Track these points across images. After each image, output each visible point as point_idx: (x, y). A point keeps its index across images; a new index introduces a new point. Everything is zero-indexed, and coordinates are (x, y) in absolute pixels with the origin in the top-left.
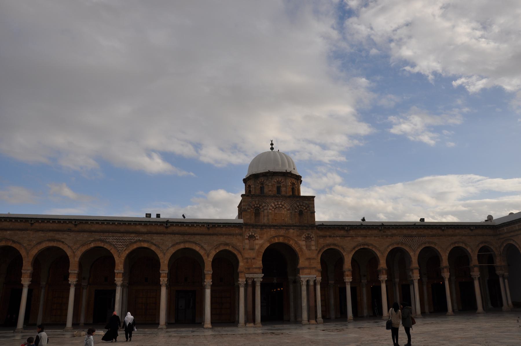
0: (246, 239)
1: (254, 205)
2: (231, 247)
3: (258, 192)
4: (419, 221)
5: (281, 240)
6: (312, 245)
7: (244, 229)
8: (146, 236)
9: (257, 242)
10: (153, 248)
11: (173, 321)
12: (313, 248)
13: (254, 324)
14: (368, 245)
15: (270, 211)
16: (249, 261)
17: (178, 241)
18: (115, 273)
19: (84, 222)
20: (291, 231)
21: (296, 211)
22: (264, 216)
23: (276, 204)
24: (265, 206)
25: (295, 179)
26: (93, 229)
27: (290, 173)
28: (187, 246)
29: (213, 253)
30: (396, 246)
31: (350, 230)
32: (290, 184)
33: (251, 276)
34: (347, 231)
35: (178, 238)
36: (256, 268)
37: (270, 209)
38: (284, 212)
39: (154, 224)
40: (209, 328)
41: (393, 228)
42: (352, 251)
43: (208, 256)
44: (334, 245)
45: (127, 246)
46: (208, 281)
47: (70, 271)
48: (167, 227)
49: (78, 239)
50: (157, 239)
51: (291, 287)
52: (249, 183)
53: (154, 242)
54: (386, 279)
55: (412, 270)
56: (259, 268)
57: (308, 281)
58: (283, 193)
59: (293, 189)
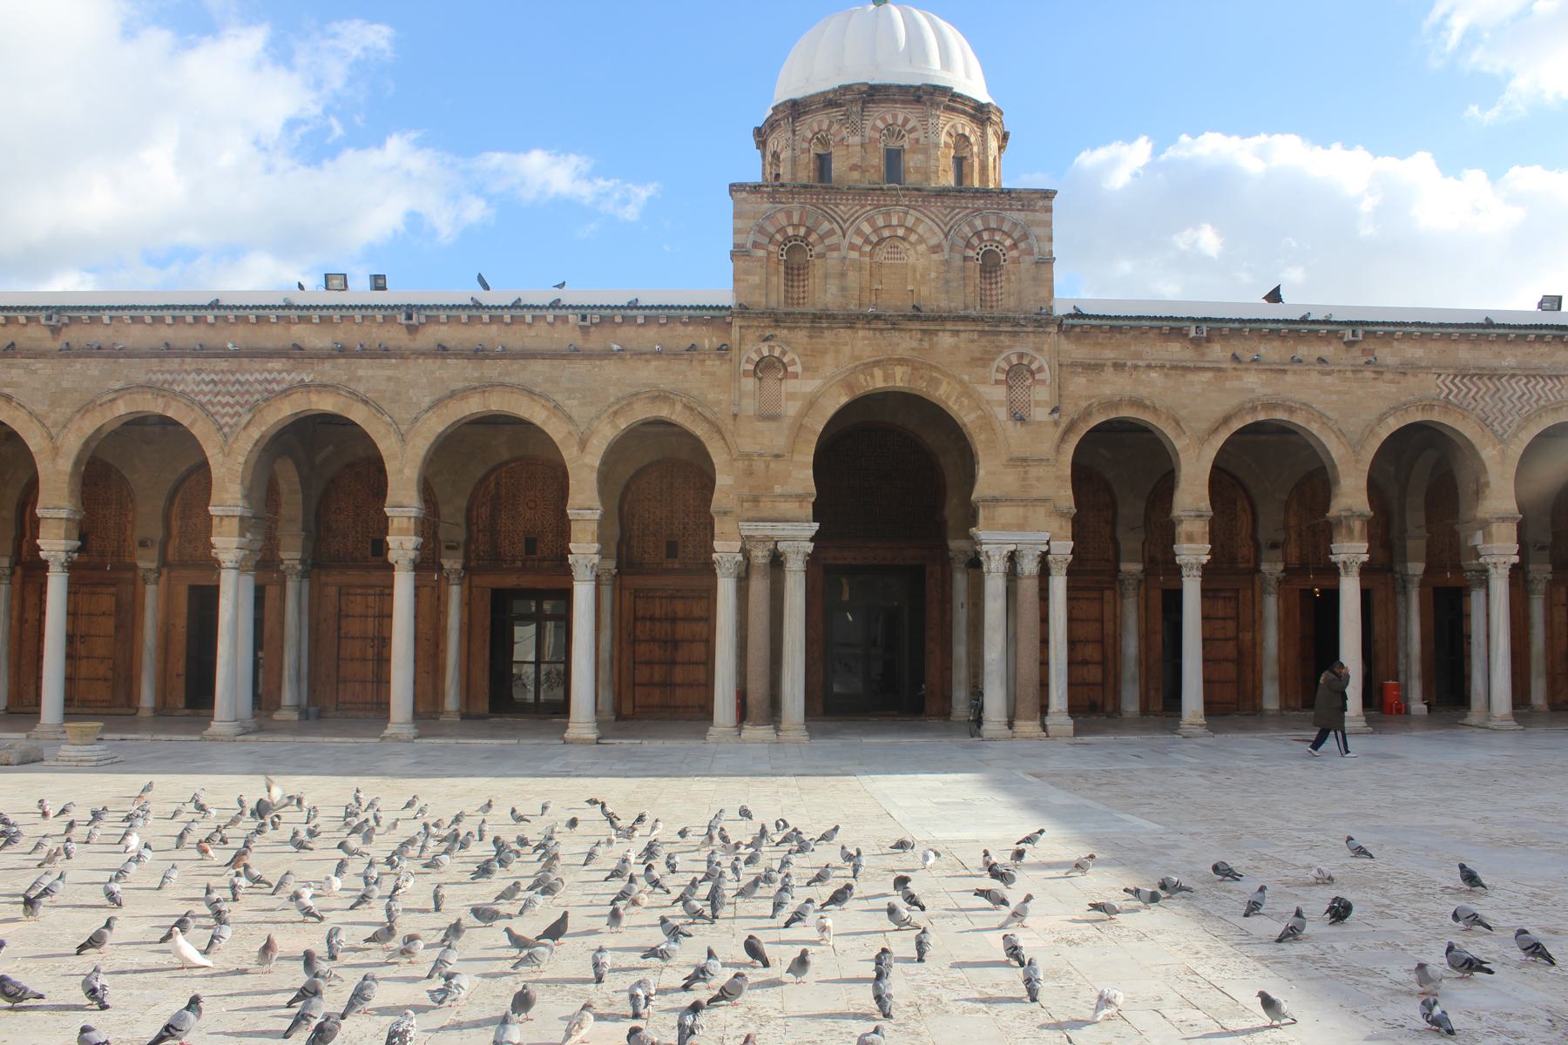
0: (746, 373)
1: (782, 230)
2: (679, 407)
3: (806, 175)
4: (1533, 307)
5: (900, 379)
6: (1038, 404)
7: (735, 333)
8: (328, 365)
9: (790, 385)
10: (358, 414)
11: (483, 705)
12: (1041, 414)
13: (777, 729)
14: (1291, 410)
15: (854, 255)
16: (759, 465)
17: (459, 385)
18: (210, 518)
19: (85, 315)
20: (945, 340)
21: (970, 253)
22: (826, 276)
23: (880, 222)
24: (831, 232)
25: (973, 117)
26: (122, 343)
27: (945, 91)
28: (497, 403)
29: (605, 434)
30: (1417, 417)
31: (1209, 340)
32: (943, 138)
33: (764, 529)
34: (1196, 342)
35: (456, 373)
36: (786, 497)
37: (852, 247)
38: (916, 257)
39: (358, 319)
40: (585, 742)
41: (1408, 336)
42: (1215, 431)
43: (583, 444)
44: (1137, 403)
45: (254, 408)
46: (585, 552)
47: (39, 512)
48: (412, 330)
49: (65, 384)
50: (371, 376)
51: (960, 581)
52: (776, 142)
53: (361, 389)
54: (1365, 558)
55: (1485, 525)
56: (800, 498)
57: (1012, 558)
58: (912, 179)
59: (960, 162)
